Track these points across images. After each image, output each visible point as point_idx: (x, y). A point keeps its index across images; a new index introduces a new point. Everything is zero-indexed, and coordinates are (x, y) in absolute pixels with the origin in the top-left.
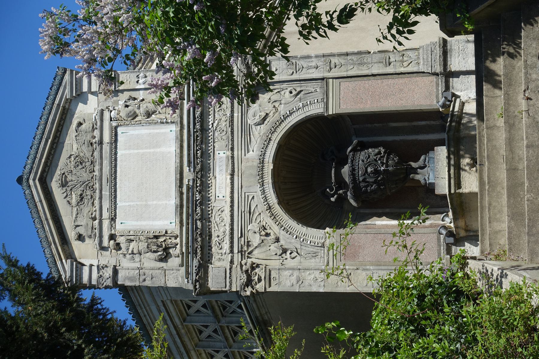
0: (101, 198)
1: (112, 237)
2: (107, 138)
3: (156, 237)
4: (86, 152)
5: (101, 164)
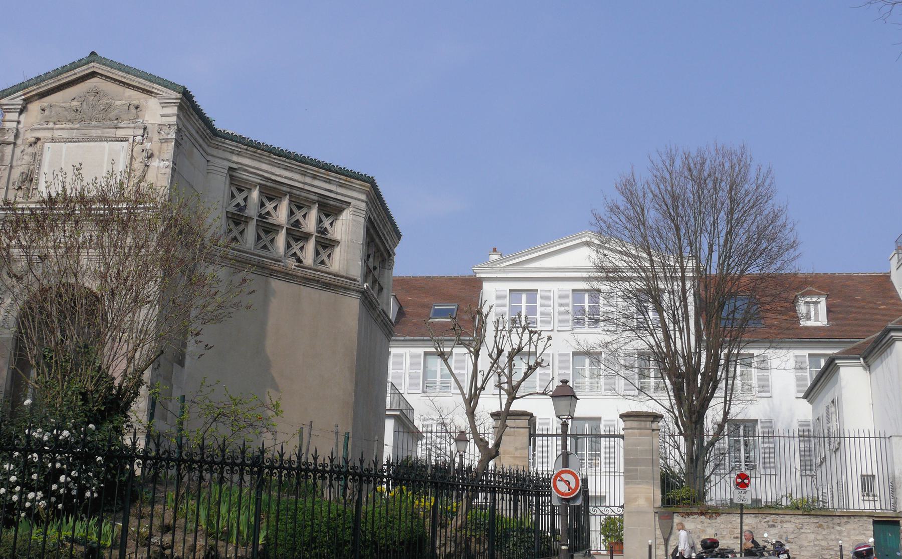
0: (71, 129)
1: (38, 139)
2: (120, 133)
3: (31, 180)
4: (113, 114)
5: (98, 128)
